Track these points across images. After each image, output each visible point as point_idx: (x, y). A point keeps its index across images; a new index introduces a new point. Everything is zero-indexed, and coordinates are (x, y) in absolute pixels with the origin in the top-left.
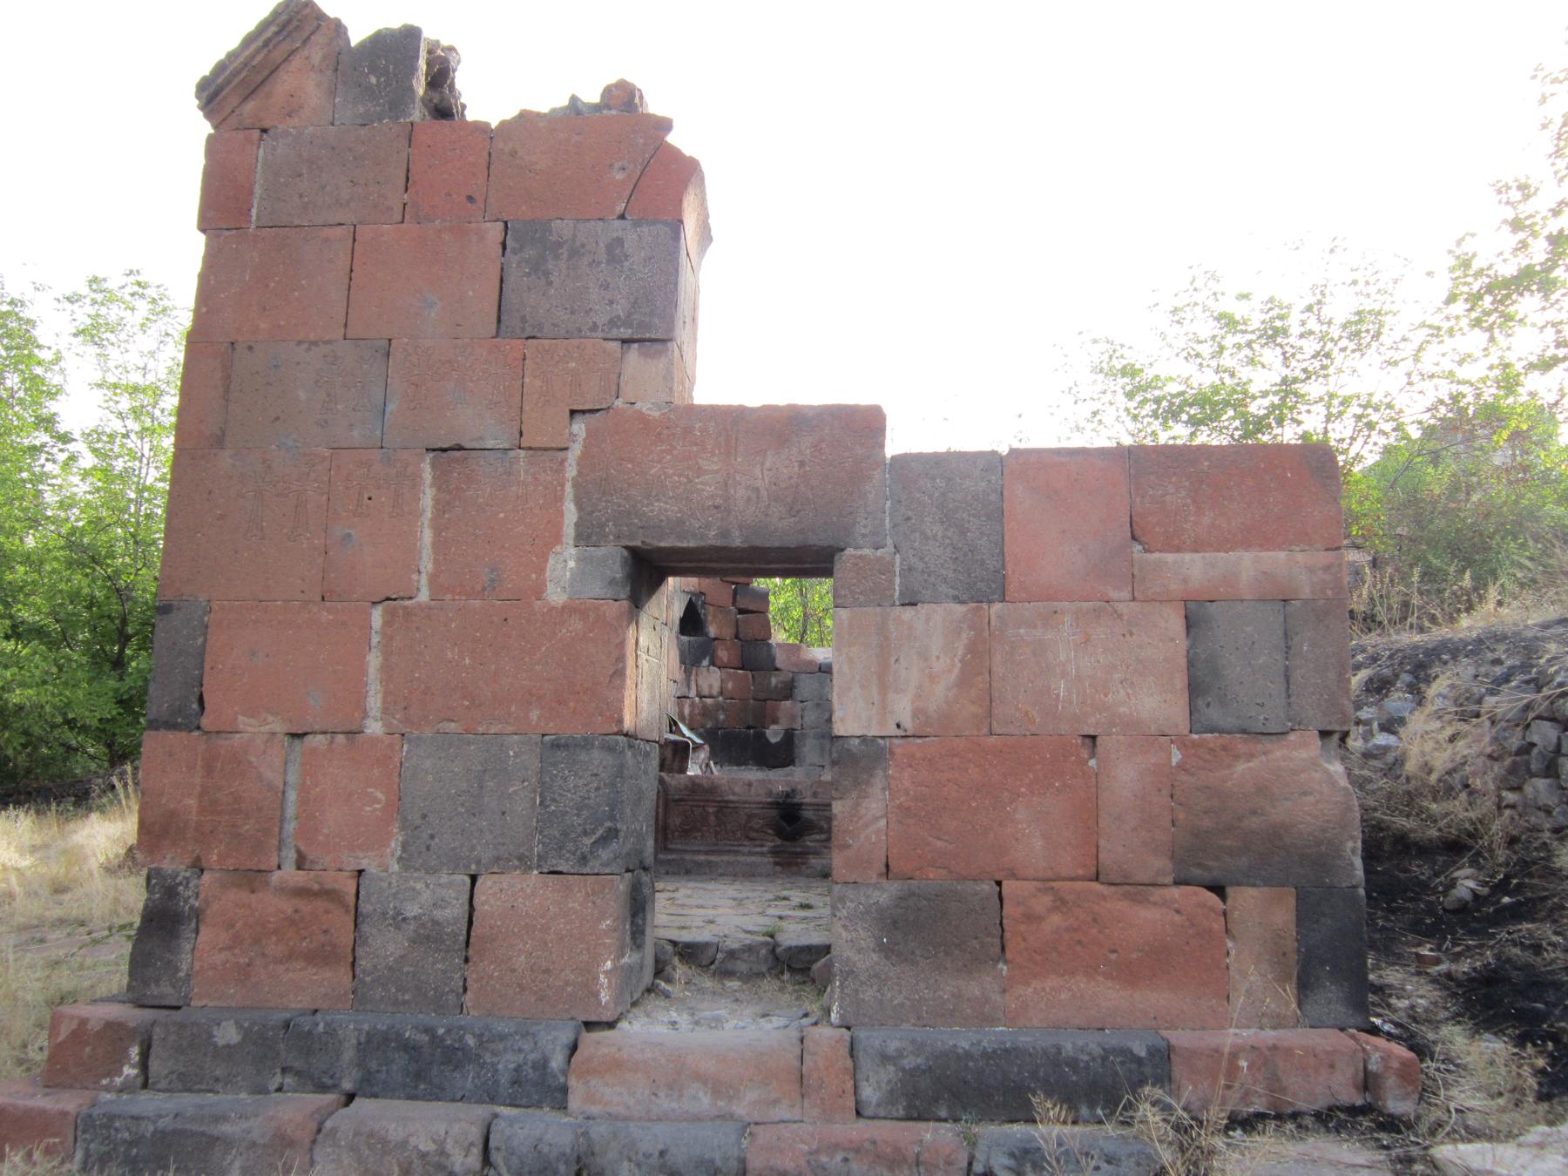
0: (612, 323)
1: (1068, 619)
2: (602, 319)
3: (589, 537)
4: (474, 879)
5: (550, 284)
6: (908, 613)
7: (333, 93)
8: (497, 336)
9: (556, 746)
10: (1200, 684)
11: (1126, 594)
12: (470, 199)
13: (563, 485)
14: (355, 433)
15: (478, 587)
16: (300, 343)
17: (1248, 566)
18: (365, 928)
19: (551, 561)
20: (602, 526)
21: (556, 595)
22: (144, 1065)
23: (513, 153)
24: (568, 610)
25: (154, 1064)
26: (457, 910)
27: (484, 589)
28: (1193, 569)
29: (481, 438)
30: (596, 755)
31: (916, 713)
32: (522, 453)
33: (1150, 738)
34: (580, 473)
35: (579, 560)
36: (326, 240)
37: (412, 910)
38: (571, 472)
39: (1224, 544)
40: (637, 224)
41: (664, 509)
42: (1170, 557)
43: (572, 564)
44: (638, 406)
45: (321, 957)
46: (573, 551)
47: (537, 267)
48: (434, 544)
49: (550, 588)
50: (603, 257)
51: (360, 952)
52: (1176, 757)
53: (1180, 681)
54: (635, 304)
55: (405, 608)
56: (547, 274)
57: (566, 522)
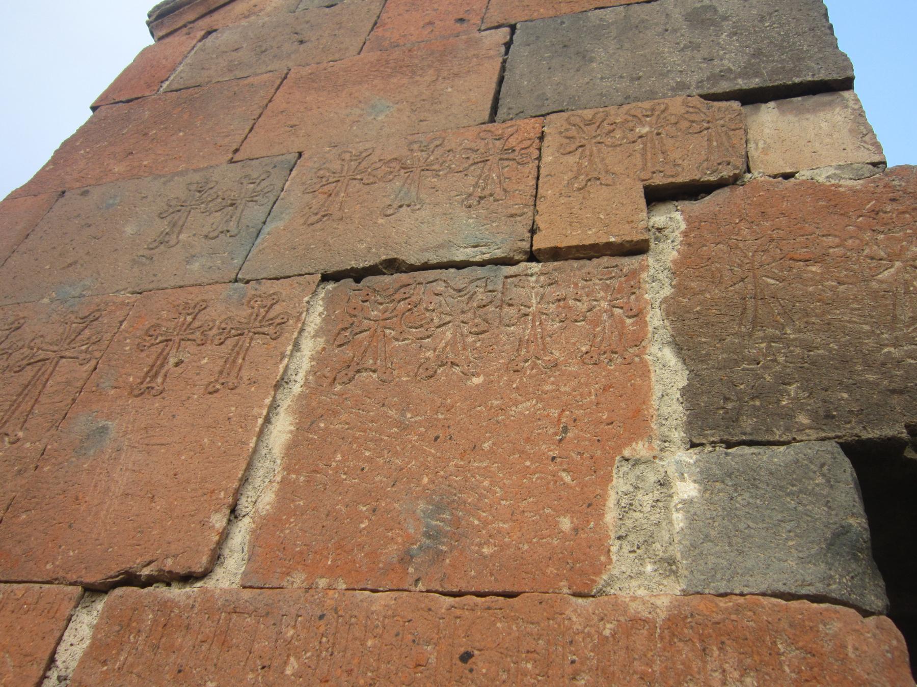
3: (733, 419)
8: (492, 120)
13: (638, 315)
14: (196, 266)
15: (392, 552)
19: (619, 484)
21: (643, 587)
27: (406, 558)
29: (441, 246)
32: (535, 267)
34: (681, 290)
35: (707, 479)
43: (687, 489)
44: (804, 174)
46: (689, 457)
48: (292, 448)
49: (621, 560)
55: (165, 606)
57: (657, 390)
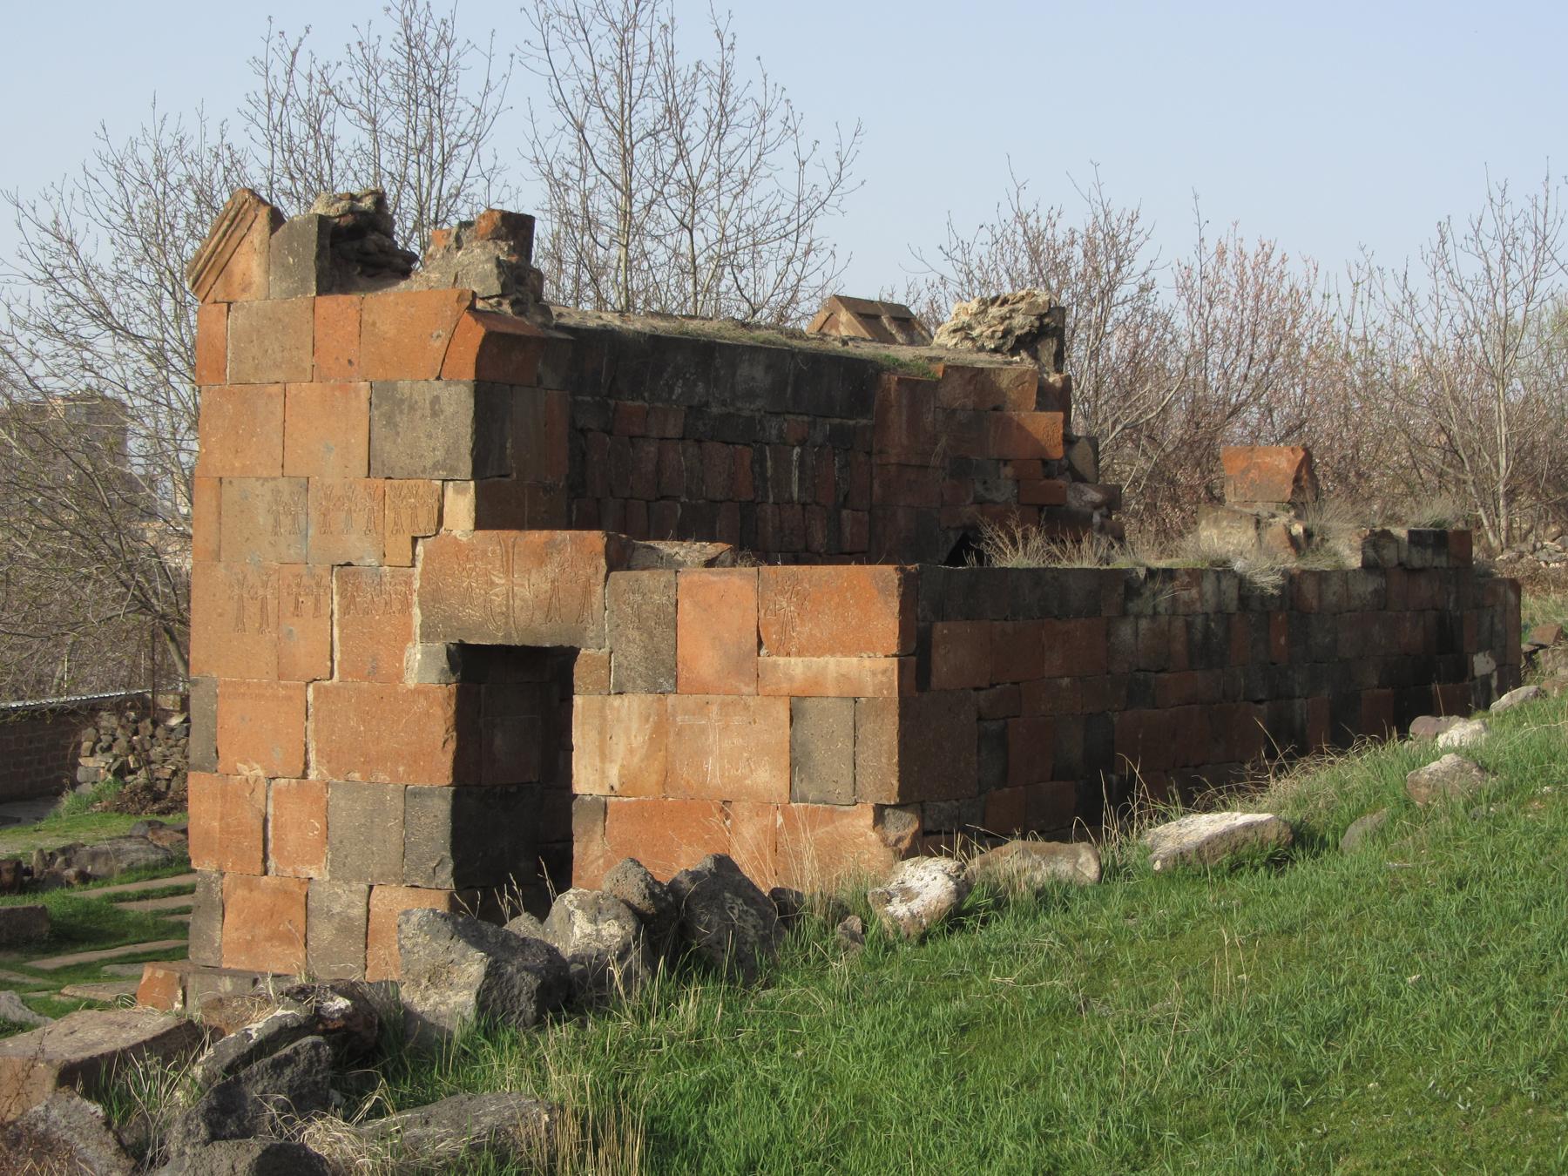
0: (435, 467)
1: (715, 709)
2: (429, 463)
4: (371, 887)
5: (398, 434)
6: (616, 701)
7: (267, 272)
9: (416, 794)
10: (798, 762)
11: (751, 689)
12: (350, 362)
16: (258, 479)
17: (834, 666)
18: (311, 919)
20: (436, 626)
21: (411, 681)
22: (184, 1001)
23: (374, 324)
24: (417, 692)
25: (189, 1001)
26: (358, 911)
28: (795, 668)
30: (436, 801)
31: (621, 776)
33: (763, 806)
36: (270, 395)
37: (337, 909)
38: (417, 585)
39: (819, 651)
40: (448, 384)
41: (473, 614)
42: (781, 660)
45: (287, 939)
47: (390, 421)
50: (428, 412)
51: (310, 936)
52: (780, 820)
53: (785, 760)
54: (447, 451)
56: (396, 425)
